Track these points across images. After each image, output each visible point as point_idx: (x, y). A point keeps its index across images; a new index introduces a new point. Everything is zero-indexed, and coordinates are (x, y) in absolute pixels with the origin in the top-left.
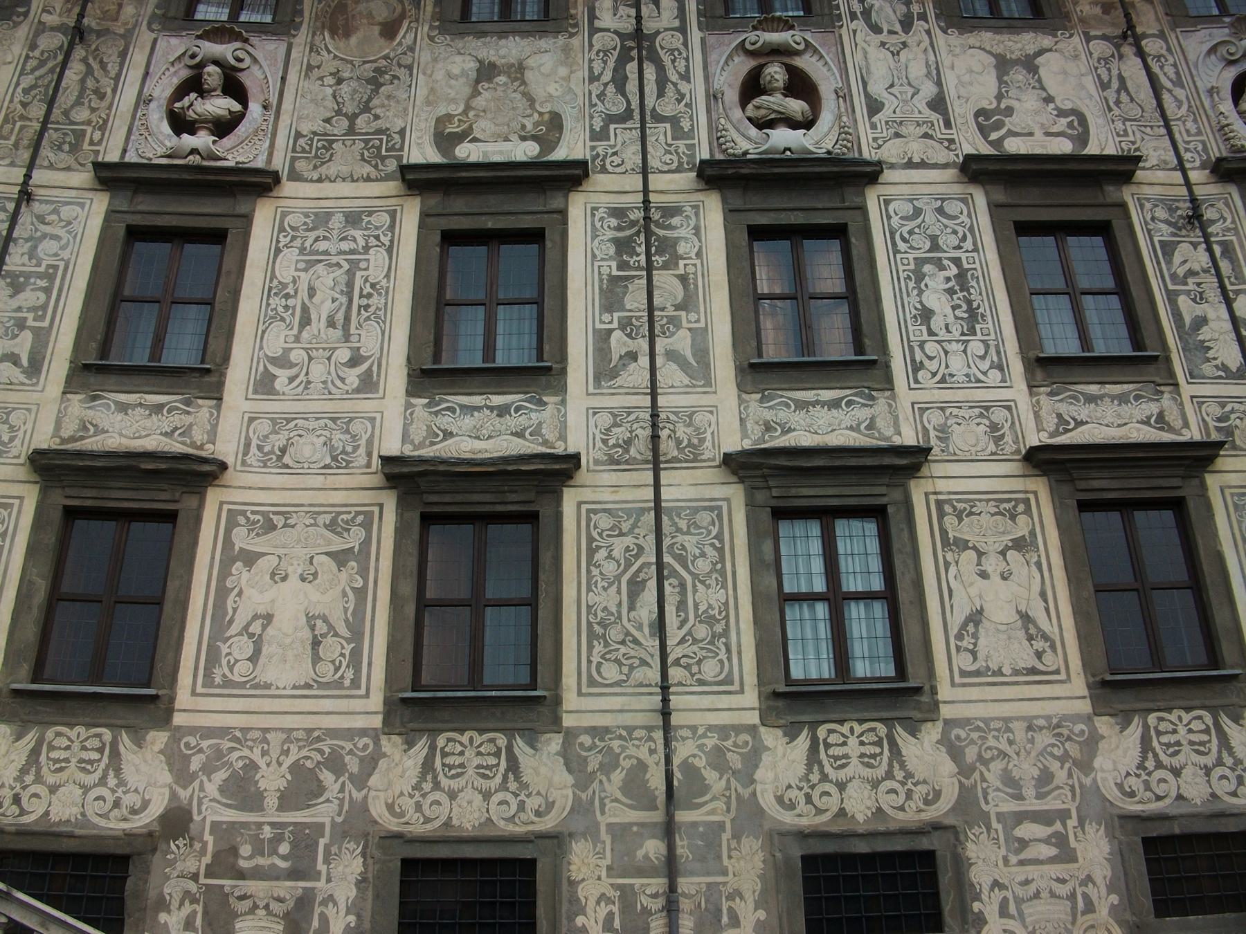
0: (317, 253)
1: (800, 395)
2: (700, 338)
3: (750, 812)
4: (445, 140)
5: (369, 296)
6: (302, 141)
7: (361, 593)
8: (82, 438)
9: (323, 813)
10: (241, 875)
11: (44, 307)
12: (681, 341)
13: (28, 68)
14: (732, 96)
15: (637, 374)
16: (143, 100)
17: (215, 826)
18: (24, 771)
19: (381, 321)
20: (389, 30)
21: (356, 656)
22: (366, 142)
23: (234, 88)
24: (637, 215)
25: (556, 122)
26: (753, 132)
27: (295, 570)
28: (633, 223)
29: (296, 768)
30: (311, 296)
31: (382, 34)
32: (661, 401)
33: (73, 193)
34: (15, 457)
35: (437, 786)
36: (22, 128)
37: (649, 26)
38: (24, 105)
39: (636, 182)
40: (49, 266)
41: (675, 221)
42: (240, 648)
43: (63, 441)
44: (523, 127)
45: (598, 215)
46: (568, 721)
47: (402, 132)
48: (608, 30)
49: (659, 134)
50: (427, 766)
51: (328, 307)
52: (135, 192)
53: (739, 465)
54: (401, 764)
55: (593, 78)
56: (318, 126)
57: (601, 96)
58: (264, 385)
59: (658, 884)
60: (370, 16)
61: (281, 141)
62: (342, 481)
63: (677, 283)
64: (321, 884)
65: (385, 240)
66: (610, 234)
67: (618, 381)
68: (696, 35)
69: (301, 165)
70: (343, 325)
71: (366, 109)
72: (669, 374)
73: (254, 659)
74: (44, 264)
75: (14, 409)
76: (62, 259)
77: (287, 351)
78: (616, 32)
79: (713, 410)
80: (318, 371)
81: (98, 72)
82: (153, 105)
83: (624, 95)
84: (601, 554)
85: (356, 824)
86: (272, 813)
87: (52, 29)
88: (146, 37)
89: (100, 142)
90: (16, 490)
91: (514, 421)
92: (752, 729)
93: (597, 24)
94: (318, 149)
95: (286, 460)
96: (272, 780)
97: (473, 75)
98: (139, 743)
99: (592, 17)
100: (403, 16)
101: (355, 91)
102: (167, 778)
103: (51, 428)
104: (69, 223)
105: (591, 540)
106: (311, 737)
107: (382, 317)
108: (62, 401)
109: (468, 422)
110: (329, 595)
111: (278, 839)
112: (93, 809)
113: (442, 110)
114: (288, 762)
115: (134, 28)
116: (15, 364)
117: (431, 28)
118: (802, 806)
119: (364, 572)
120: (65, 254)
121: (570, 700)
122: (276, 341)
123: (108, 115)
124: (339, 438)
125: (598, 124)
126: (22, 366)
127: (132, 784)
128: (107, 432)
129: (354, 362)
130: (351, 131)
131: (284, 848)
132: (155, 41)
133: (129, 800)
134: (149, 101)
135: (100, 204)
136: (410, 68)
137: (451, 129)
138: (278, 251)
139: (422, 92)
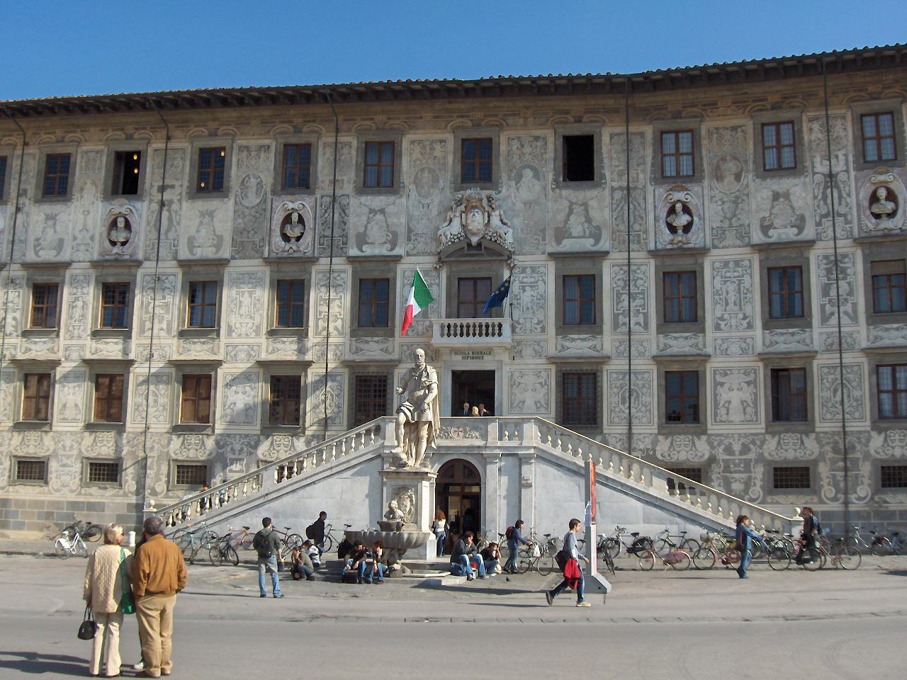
0: (726, 277)
1: (887, 326)
2: (855, 305)
3: (867, 456)
4: (765, 229)
5: (746, 294)
6: (714, 231)
7: (755, 394)
9: (751, 456)
10: (731, 472)
11: (644, 304)
12: (849, 307)
14: (866, 204)
15: (834, 320)
16: (656, 219)
17: (723, 460)
18: (670, 448)
19: (751, 303)
20: (738, 177)
21: (756, 413)
22: (736, 230)
23: (686, 210)
24: (833, 258)
25: (802, 218)
26: (873, 220)
27: (735, 387)
28: (832, 262)
29: (743, 444)
30: (727, 294)
31: (735, 179)
32: (842, 329)
33: (641, 261)
35: (782, 448)
37: (835, 170)
38: (617, 225)
39: (831, 244)
41: (846, 260)
42: (723, 411)
43: (661, 351)
44: (791, 221)
45: (820, 258)
46: (817, 430)
47: (749, 225)
48: (818, 173)
49: (839, 220)
50: (779, 443)
51: (733, 298)
53: (867, 351)
54: (771, 444)
55: (815, 197)
56: (719, 224)
57: (818, 206)
58: (717, 327)
59: (842, 473)
60: (729, 170)
61: (708, 232)
62: (746, 359)
63: (846, 285)
64: (753, 474)
65: (749, 271)
66: (825, 266)
67: (828, 323)
68: (853, 173)
69: (716, 242)
70: (739, 304)
71: (735, 215)
72: (845, 320)
73: (727, 414)
77: (723, 315)
78: (822, 174)
79: (858, 332)
80: (733, 322)
81: (638, 208)
83: (827, 205)
84: (825, 381)
85: (761, 459)
86: (737, 457)
87: (617, 189)
88: (650, 189)
89: (646, 239)
90: (651, 367)
91: (797, 337)
92: (868, 432)
93: (816, 170)
94: (719, 234)
95: (728, 352)
96: (737, 447)
97: (771, 197)
98: (699, 438)
99: (813, 167)
100: (742, 171)
101: (729, 208)
102: (708, 448)
105: (822, 376)
106: (746, 436)
107: (751, 302)
109: (782, 338)
110: (746, 394)
111: (740, 463)
112: (690, 457)
113: (762, 215)
114: (740, 443)
117: (753, 176)
118: (882, 453)
119: (756, 387)
121: (818, 424)
122: (718, 314)
124: (743, 345)
125: (818, 219)
127: (700, 449)
129: (745, 318)
130: (731, 226)
131: (742, 465)
133: (699, 454)
135: (652, 262)
136: (747, 195)
137: (766, 223)
138: (714, 278)
139: (754, 207)
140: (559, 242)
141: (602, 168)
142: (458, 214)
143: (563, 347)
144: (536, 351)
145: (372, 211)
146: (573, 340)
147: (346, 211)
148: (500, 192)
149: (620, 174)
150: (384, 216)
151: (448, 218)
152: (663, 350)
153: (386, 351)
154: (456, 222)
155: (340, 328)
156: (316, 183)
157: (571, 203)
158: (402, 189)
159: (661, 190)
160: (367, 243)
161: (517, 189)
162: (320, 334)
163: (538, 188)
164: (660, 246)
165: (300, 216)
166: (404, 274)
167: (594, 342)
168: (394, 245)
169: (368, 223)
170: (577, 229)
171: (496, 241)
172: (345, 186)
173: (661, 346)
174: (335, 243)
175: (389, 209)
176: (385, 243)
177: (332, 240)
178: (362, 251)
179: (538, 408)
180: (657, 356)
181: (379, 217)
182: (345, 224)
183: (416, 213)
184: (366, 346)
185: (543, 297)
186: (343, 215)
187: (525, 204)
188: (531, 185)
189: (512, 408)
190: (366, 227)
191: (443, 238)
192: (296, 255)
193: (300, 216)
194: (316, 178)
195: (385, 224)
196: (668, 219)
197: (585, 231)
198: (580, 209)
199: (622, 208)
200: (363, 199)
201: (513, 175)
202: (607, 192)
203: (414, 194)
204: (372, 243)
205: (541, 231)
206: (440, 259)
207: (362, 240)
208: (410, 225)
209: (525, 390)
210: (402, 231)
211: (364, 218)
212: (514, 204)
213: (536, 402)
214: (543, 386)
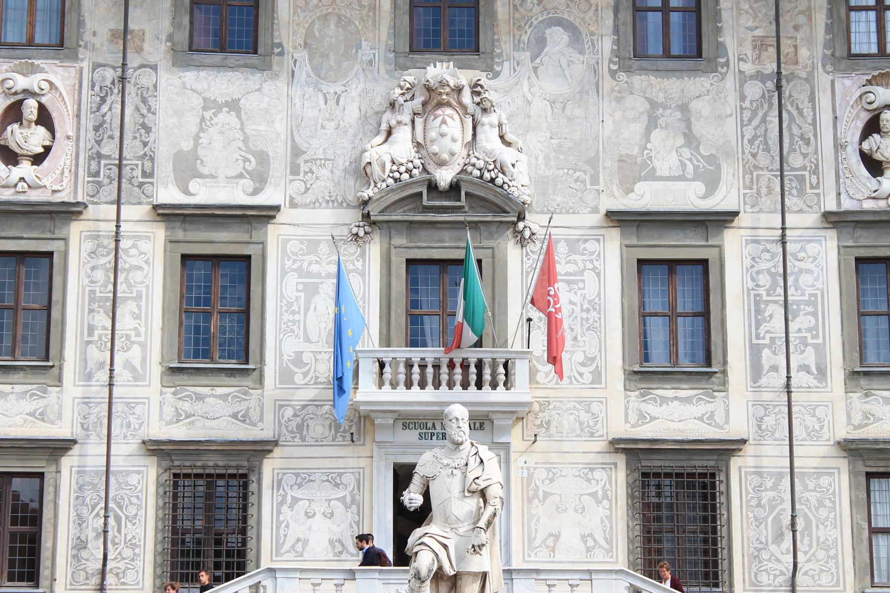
8: (867, 425)
11: (816, 327)
13: (746, 119)
16: (839, 146)
34: (827, 440)
36: (758, 177)
38: (754, 156)
40: (811, 295)
43: (856, 428)
52: (855, 227)
74: (807, 293)
75: (817, 406)
76: (818, 289)
81: (798, 120)
82: (849, 149)
87: (752, 77)
88: (823, 79)
103: (844, 418)
104: (815, 259)
108: (847, 399)
115: (813, 68)
116: (808, 372)
120: (819, 285)
123: (817, 160)
126: (813, 374)
128: (882, 419)
132: (833, 82)
134: (844, 147)
140: (629, 191)
141: (718, 31)
142: (406, 118)
143: (642, 416)
144: (581, 424)
145: (208, 104)
146: (664, 400)
147: (151, 101)
148: (497, 75)
149: (760, 45)
150: (239, 117)
151: (384, 127)
152: (861, 426)
153: (243, 418)
154: (403, 138)
155: (137, 364)
156: (79, 36)
157: (653, 104)
158: (275, 59)
159: (848, 82)
160: (201, 176)
161: (535, 69)
162: (89, 377)
164: (847, 205)
165: (42, 108)
166: (284, 248)
167: (710, 407)
168: (261, 180)
169: (202, 130)
170: (667, 163)
171: (492, 180)
172: (147, 46)
173: (857, 419)
174: (126, 171)
175: (249, 103)
176: (241, 176)
177: (120, 166)
178: (187, 192)
179: (588, 550)
180: (852, 441)
181: (226, 118)
182: (148, 130)
183: (310, 113)
184: (198, 407)
185: (594, 306)
186: (145, 111)
187: (552, 103)
188: (564, 63)
189: (531, 548)
190: (197, 138)
191: (376, 169)
192: (34, 196)
193: (42, 108)
194: (81, 23)
195: (239, 135)
196: (866, 146)
197: (683, 166)
198: (672, 116)
199: (764, 120)
200: (190, 76)
201: (525, 38)
202: (730, 83)
203: (304, 71)
204: (211, 176)
205: (587, 162)
206: (366, 217)
207: (188, 168)
208: (297, 139)
209: (560, 509)
210: (279, 153)
211: (192, 122)
212: (530, 103)
213: (584, 538)
214: (598, 502)
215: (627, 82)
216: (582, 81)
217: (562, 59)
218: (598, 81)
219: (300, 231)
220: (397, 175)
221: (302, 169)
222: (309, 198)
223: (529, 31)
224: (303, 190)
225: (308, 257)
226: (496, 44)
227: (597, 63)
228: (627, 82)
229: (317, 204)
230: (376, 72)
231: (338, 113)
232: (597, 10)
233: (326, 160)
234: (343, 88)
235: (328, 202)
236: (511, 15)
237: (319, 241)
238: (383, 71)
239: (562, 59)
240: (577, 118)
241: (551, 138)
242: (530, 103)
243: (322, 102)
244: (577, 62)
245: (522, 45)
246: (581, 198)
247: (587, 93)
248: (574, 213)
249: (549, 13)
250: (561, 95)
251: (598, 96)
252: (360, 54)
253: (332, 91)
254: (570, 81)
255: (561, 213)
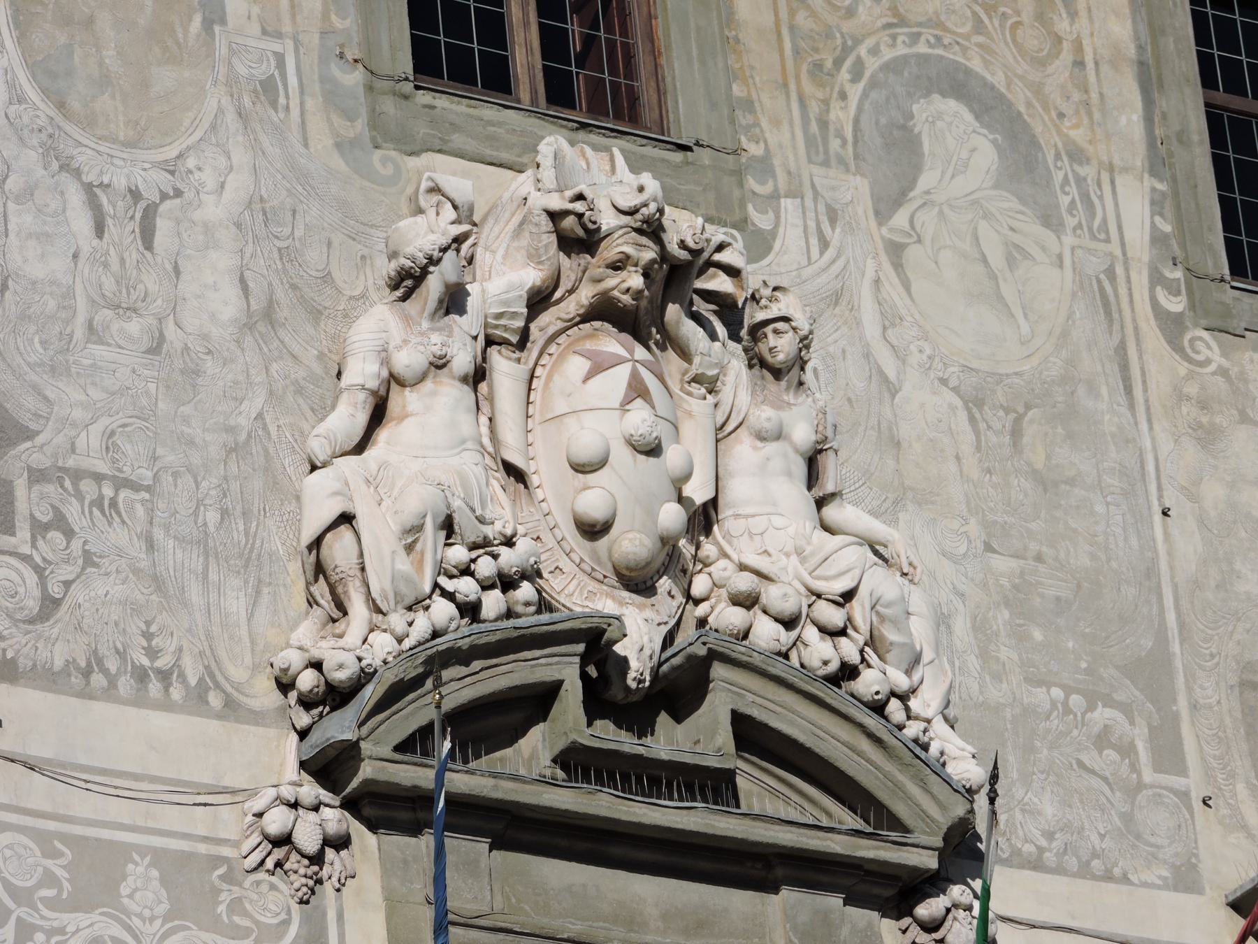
151: (363, 372)
161: (896, 251)
163: (1050, 284)
187: (974, 403)
201: (842, 116)
215: (1223, 372)
216: (1065, 334)
217: (983, 226)
218: (1122, 349)
219: (38, 792)
220: (466, 587)
221: (21, 506)
222: (59, 647)
223: (855, 92)
224: (33, 604)
225: (82, 919)
226: (744, 119)
227: (1111, 273)
228: (1223, 372)
229: (98, 680)
230: (294, 137)
231: (151, 281)
232: (1080, 64)
233: (122, 483)
234: (163, 180)
235: (141, 676)
236: (784, 14)
237: (124, 852)
238: (321, 139)
239: (983, 226)
240: (1071, 482)
241: (989, 548)
242: (892, 390)
243: (81, 222)
244: (1035, 251)
245: (835, 144)
246: (1128, 818)
247: (1093, 390)
248: (1108, 877)
249: (915, 38)
250: (1000, 378)
251: (1132, 406)
252: (221, 49)
253: (121, 182)
254: (1025, 328)
255: (1059, 870)
